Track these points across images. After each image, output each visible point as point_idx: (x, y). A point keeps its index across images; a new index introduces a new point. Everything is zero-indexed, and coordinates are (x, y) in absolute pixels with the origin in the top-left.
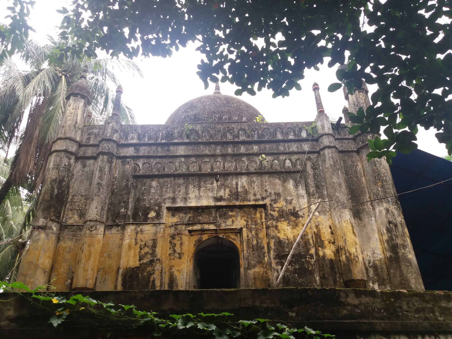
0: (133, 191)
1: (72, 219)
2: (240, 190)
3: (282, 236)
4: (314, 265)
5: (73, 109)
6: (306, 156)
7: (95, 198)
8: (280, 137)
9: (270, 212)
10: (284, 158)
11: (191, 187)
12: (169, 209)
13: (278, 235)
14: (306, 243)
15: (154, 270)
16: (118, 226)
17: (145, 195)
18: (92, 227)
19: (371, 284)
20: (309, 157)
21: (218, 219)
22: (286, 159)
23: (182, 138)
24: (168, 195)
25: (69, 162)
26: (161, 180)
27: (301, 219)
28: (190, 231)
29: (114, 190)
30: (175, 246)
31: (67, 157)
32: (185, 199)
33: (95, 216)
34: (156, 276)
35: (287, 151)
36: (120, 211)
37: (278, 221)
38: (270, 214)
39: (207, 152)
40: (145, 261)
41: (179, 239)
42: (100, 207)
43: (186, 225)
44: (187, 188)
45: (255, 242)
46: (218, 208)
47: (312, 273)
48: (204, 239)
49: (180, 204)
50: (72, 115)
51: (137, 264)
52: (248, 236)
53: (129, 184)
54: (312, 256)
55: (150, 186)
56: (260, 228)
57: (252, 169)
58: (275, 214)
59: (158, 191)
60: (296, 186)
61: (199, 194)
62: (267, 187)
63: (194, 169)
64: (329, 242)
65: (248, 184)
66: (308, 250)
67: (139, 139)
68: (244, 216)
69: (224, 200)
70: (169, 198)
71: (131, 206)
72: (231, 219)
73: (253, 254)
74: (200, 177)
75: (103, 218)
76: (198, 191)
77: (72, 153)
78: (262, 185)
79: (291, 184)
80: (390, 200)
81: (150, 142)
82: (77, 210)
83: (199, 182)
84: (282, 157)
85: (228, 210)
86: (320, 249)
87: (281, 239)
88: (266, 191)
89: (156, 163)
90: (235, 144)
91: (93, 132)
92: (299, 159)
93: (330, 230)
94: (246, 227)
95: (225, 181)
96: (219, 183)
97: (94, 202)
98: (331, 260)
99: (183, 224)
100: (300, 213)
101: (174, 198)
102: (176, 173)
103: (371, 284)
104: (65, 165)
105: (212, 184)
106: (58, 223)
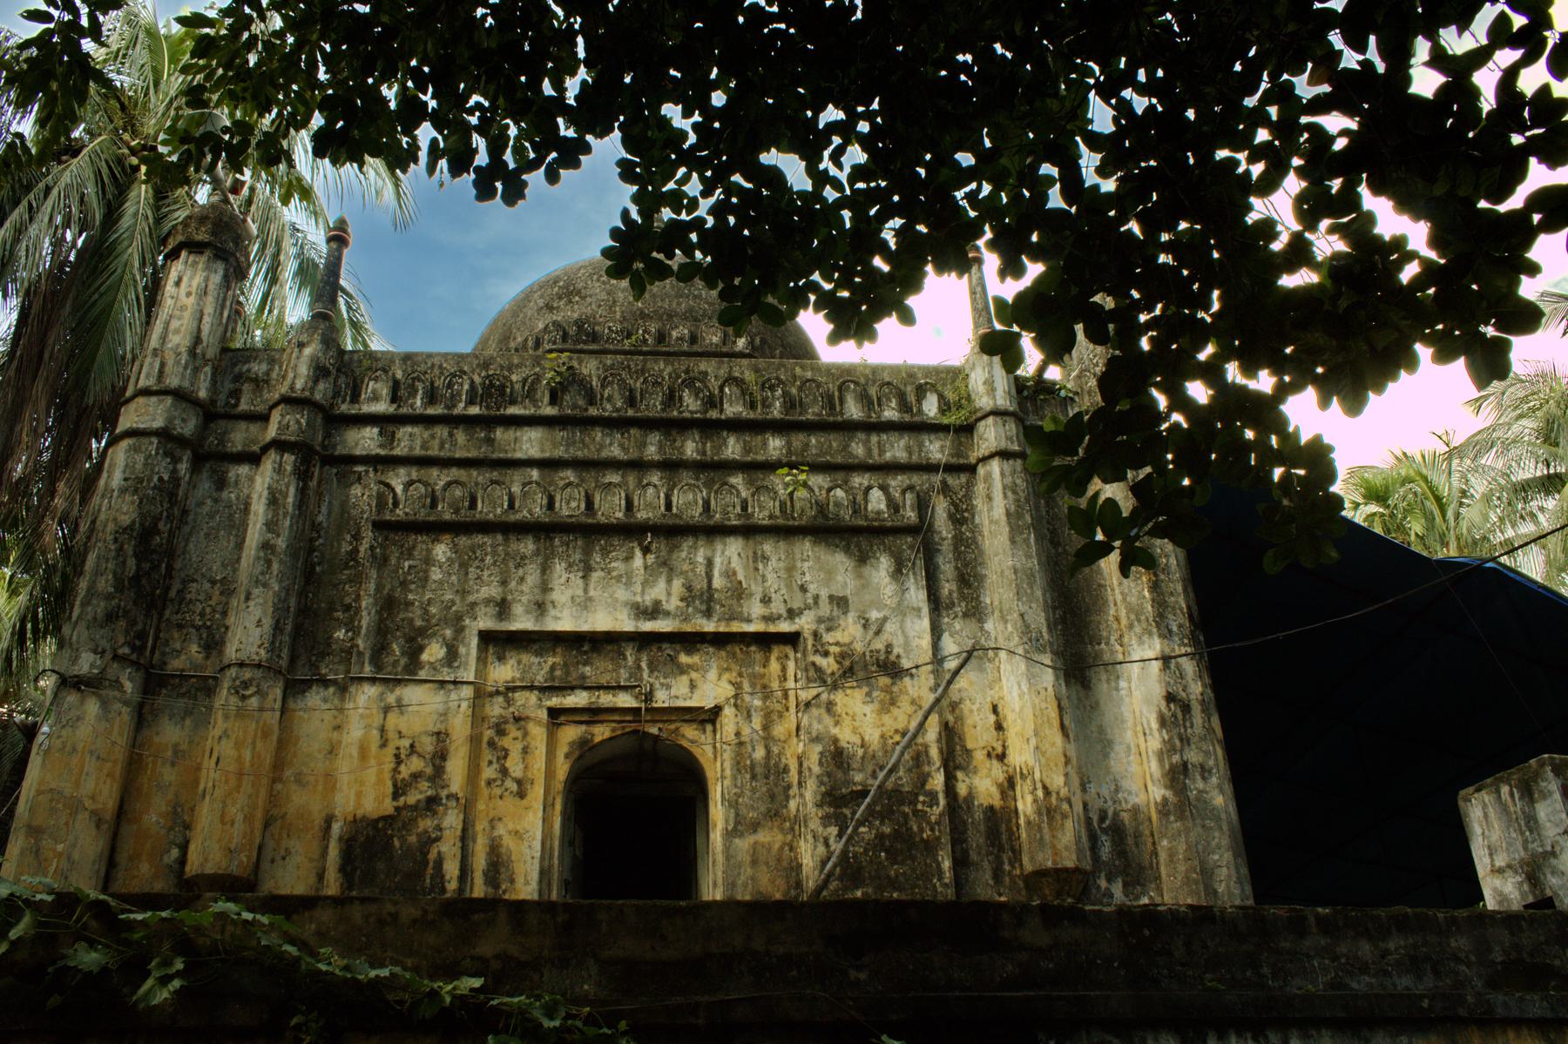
0: (374, 574)
1: (183, 657)
2: (718, 582)
3: (845, 736)
4: (938, 823)
5: (189, 294)
6: (937, 479)
7: (256, 591)
8: (853, 410)
9: (812, 658)
10: (866, 483)
11: (559, 567)
12: (487, 637)
13: (835, 731)
14: (920, 758)
15: (439, 828)
16: (325, 683)
17: (413, 587)
18: (246, 685)
19: (1103, 883)
20: (944, 482)
21: (645, 675)
22: (870, 488)
23: (535, 402)
24: (485, 592)
25: (175, 471)
26: (463, 541)
27: (907, 680)
28: (554, 713)
29: (313, 567)
30: (505, 757)
31: (166, 454)
32: (540, 607)
33: (255, 649)
34: (448, 848)
35: (876, 458)
36: (331, 637)
37: (835, 687)
38: (814, 664)
39: (616, 452)
40: (412, 798)
41: (519, 734)
42: (268, 622)
43: (542, 689)
44: (545, 569)
45: (759, 754)
46: (645, 641)
47: (930, 847)
48: (598, 739)
49: (522, 622)
50: (187, 314)
51: (388, 807)
52: (738, 734)
53: (362, 549)
54: (933, 795)
55: (429, 561)
56: (778, 707)
57: (761, 516)
59: (454, 578)
60: (898, 573)
61: (586, 591)
62: (808, 577)
63: (569, 507)
64: (989, 755)
65: (746, 568)
66: (924, 779)
67: (394, 399)
68: (728, 669)
69: (667, 614)
70: (488, 601)
71: (366, 620)
72: (685, 679)
73: (754, 790)
74: (591, 535)
75: (279, 656)
76: (580, 582)
77: (182, 441)
78: (790, 569)
79: (882, 568)
80: (1175, 629)
81: (430, 411)
82: (198, 629)
83: (587, 553)
84: (859, 480)
85: (678, 647)
86: (960, 775)
87: (844, 745)
88: (803, 589)
89: (449, 484)
90: (710, 428)
91: (249, 370)
92: (911, 488)
93: (992, 718)
94: (736, 705)
95: (671, 551)
96: (651, 558)
97: (252, 603)
98: (991, 808)
99: (531, 688)
101: (504, 600)
102: (512, 518)
103: (1103, 883)
104: (161, 479)
105: (629, 558)
106: (136, 664)
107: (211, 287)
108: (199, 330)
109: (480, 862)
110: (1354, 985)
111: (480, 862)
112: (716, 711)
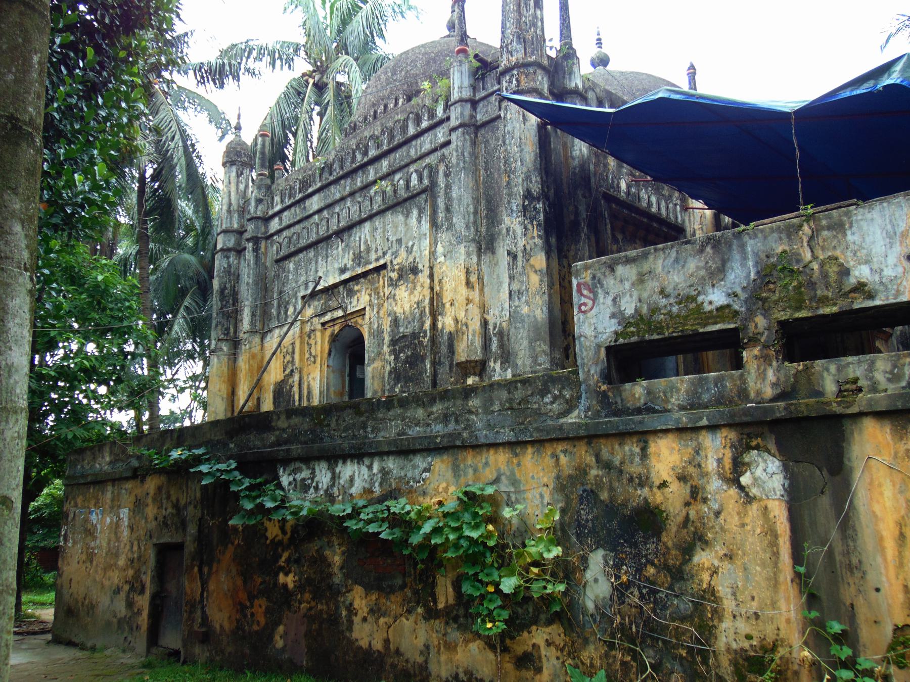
13: (395, 309)
28: (323, 324)
34: (296, 389)
42: (249, 314)
44: (317, 262)
45: (375, 326)
46: (345, 282)
58: (394, 275)
80: (515, 208)
86: (440, 318)
88: (388, 240)
99: (316, 316)
100: (420, 267)
103: (492, 364)
107: (232, 179)
108: (230, 200)
109: (305, 392)
110: (410, 433)
111: (305, 392)
112: (364, 309)
